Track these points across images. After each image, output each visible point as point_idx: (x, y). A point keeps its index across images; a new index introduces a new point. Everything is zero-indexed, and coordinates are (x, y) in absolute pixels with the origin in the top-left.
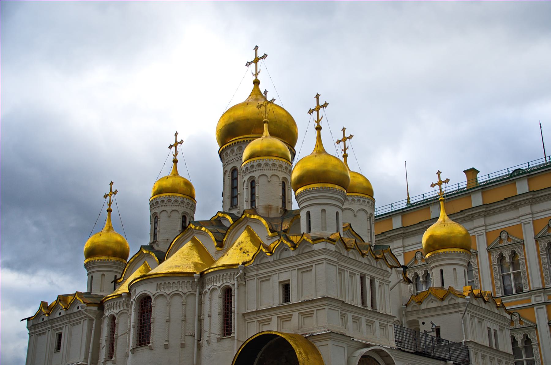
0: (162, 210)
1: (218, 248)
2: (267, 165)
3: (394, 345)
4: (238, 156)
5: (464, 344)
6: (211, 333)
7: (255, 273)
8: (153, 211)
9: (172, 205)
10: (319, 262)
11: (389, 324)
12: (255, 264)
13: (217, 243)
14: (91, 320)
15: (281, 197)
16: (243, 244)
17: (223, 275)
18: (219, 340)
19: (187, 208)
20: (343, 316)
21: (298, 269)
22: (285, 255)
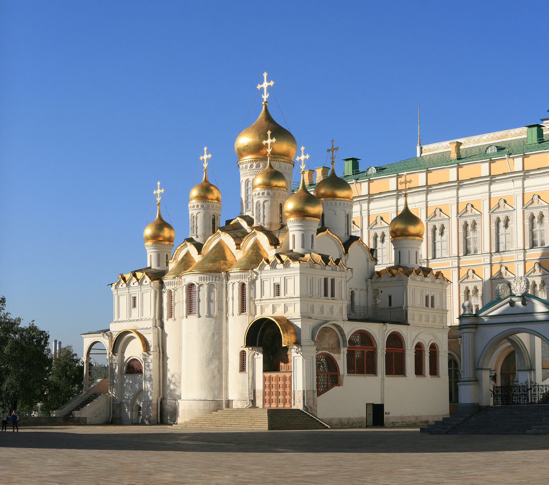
1: (238, 250)
3: (346, 317)
14: (156, 292)
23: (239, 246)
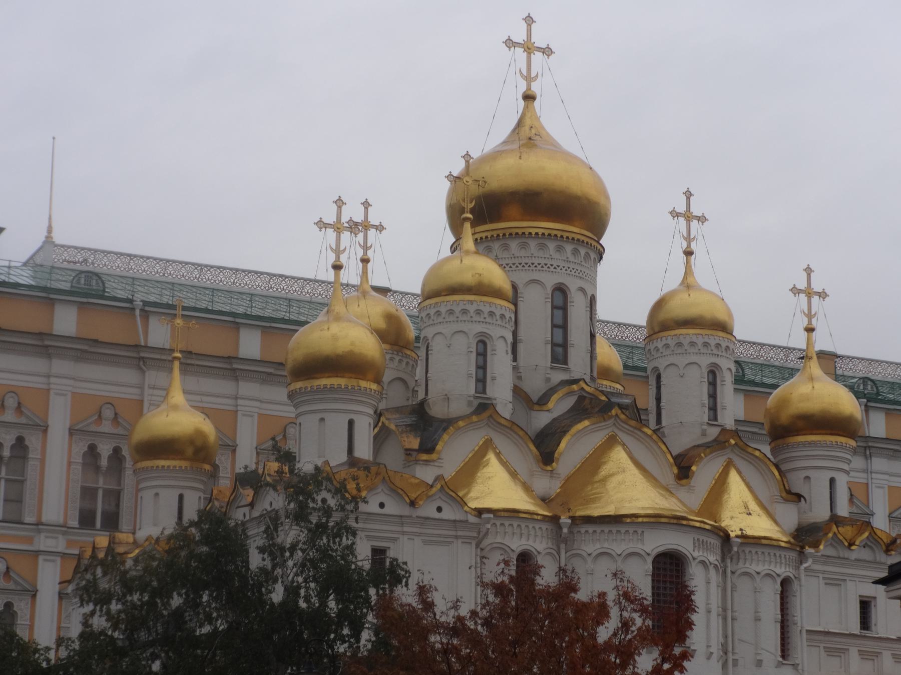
4: (572, 266)
6: (762, 649)
8: (479, 328)
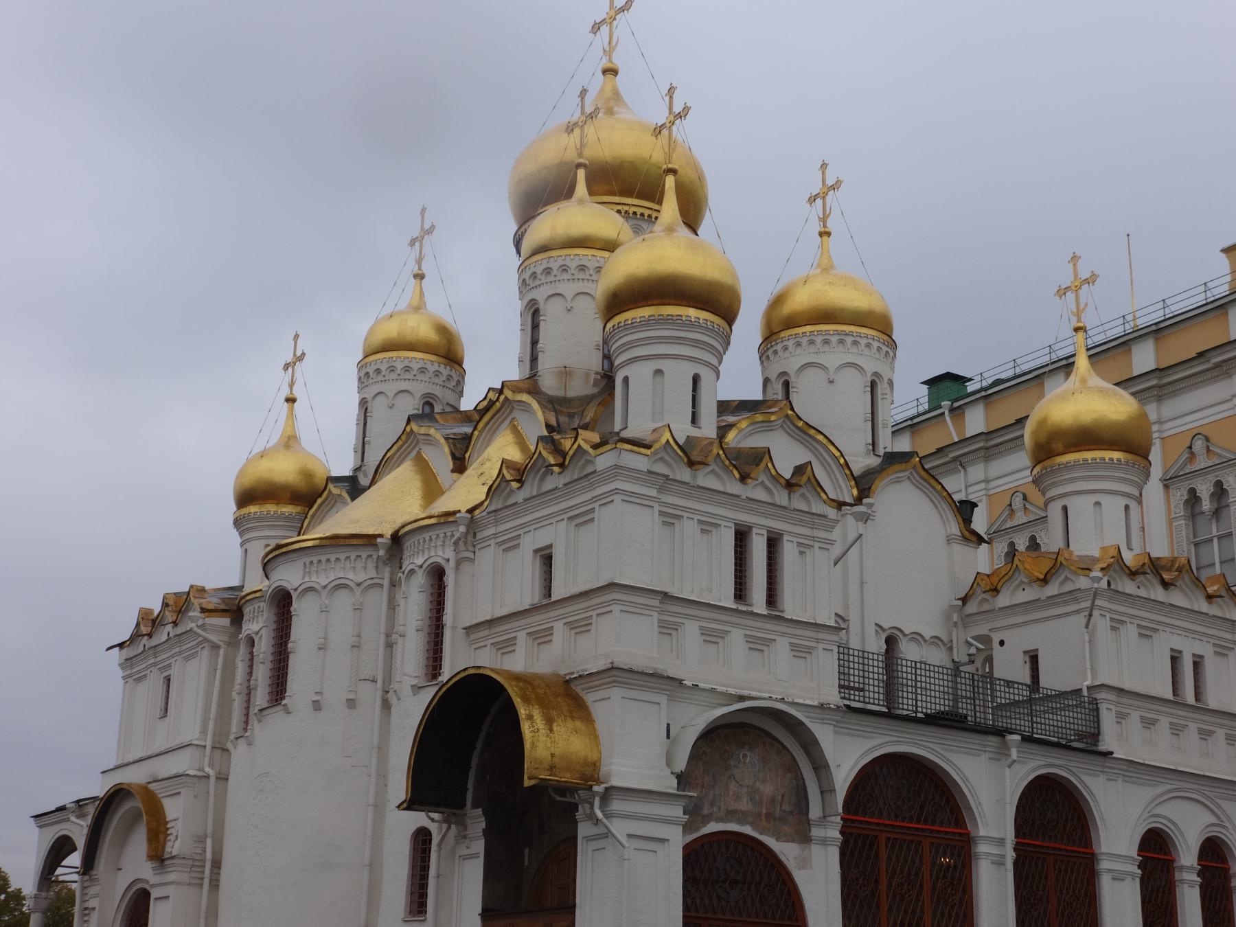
0: (376, 393)
2: (564, 268)
3: (833, 697)
5: (1085, 693)
6: (405, 674)
7: (492, 531)
9: (397, 380)
10: (605, 500)
11: (821, 646)
12: (492, 508)
13: (454, 463)
14: (215, 647)
15: (598, 345)
16: (490, 463)
17: (431, 539)
18: (417, 689)
19: (434, 383)
20: (667, 629)
21: (569, 518)
22: (550, 483)
23: (459, 462)
